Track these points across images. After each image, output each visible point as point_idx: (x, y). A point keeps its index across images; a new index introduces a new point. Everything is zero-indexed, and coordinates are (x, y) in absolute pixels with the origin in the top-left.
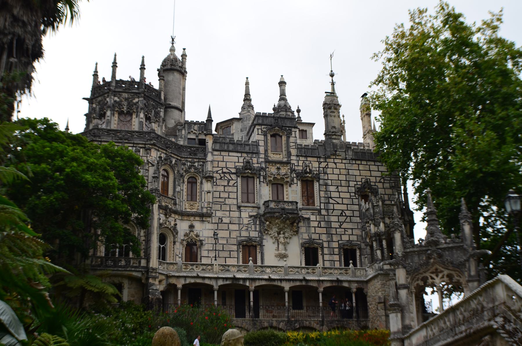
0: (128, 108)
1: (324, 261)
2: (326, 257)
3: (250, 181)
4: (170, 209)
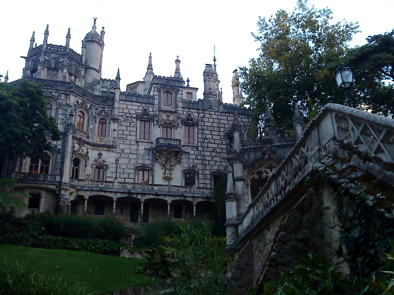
0: (55, 65)
1: (199, 183)
2: (201, 181)
3: (147, 124)
4: (83, 141)
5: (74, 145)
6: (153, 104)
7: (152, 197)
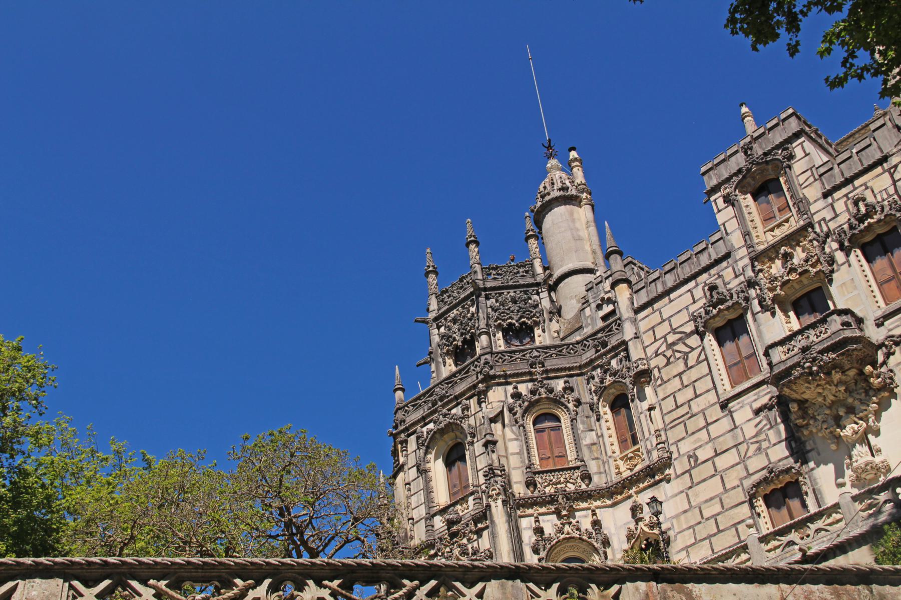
0: (462, 334)
4: (568, 497)
5: (542, 525)
6: (727, 256)
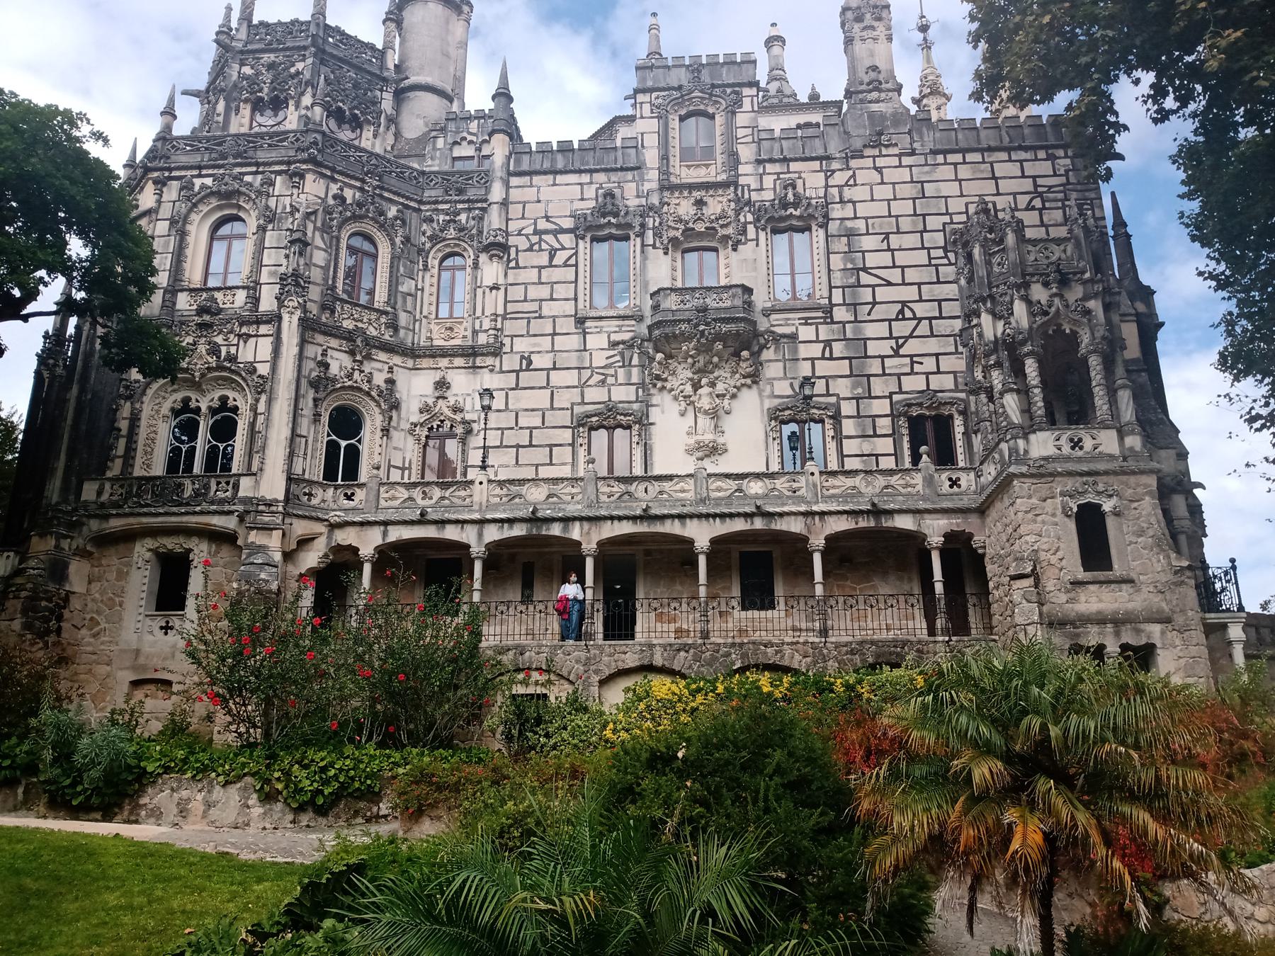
1: (842, 456)
5: (329, 361)
7: (626, 528)
